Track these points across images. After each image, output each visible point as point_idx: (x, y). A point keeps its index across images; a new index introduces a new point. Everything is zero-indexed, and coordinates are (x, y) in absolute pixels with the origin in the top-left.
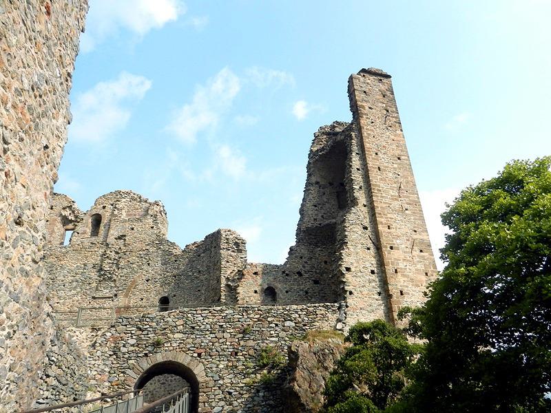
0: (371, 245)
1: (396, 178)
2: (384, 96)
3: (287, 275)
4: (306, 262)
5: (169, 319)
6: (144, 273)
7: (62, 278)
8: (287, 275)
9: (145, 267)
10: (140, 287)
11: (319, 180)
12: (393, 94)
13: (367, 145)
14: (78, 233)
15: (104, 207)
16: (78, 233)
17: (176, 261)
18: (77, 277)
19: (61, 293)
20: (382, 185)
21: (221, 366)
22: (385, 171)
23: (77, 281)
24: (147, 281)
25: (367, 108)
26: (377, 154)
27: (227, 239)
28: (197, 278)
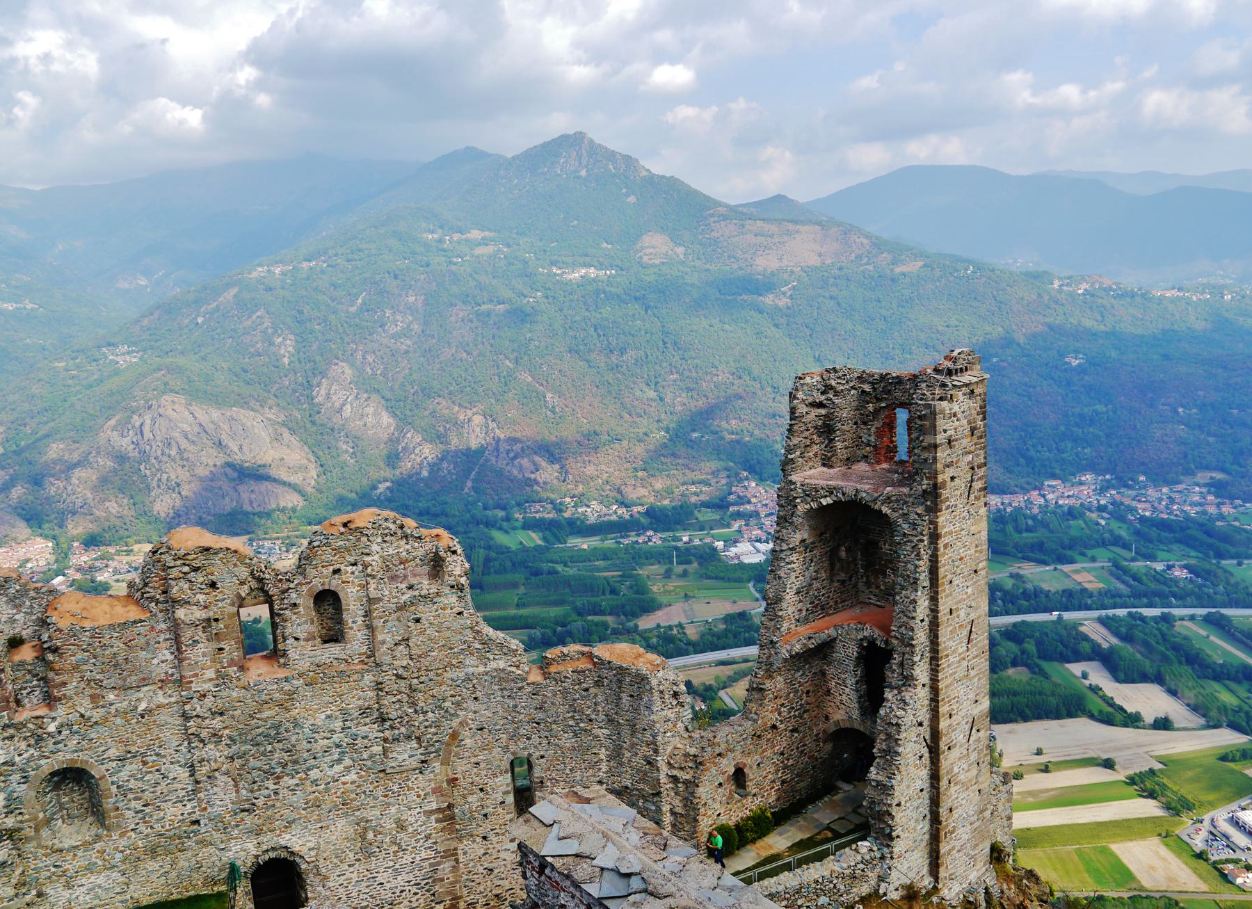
0: (925, 752)
3: (759, 737)
4: (782, 705)
6: (471, 715)
7: (306, 746)
9: (472, 705)
11: (806, 536)
13: (942, 571)
14: (297, 639)
16: (297, 639)
18: (336, 738)
19: (314, 774)
22: (958, 609)
23: (338, 746)
24: (481, 729)
27: (662, 692)
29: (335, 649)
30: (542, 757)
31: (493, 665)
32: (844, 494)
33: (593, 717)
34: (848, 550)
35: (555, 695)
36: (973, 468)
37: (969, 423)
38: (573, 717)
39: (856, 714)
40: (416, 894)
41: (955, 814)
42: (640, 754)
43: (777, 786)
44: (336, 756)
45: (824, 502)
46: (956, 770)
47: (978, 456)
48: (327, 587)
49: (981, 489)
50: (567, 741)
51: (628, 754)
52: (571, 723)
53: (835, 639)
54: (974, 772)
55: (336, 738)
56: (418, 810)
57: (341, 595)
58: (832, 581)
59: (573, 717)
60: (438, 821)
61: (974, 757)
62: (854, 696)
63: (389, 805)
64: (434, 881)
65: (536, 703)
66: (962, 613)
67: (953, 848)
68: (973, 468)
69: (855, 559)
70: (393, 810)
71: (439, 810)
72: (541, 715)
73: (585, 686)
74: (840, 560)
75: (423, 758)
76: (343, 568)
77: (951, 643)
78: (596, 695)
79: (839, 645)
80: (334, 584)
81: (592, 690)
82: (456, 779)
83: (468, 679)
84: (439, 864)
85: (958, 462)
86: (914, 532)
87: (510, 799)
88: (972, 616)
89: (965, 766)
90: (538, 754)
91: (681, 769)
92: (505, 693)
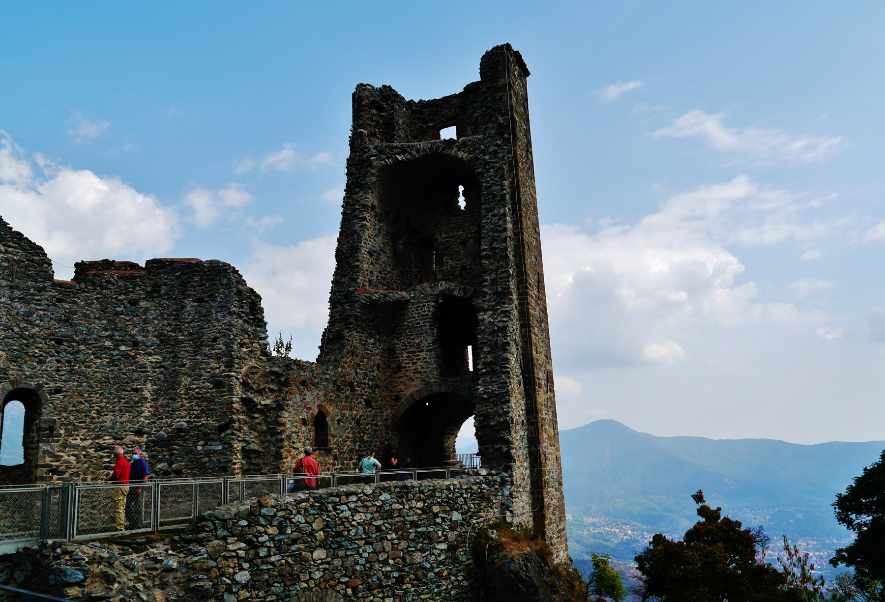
5: (300, 518)
17: (59, 300)
28: (126, 356)
30: (58, 391)
32: (418, 151)
33: (140, 338)
35: (90, 305)
42: (206, 375)
50: (99, 366)
52: (108, 343)
53: (409, 301)
59: (111, 337)
65: (60, 313)
72: (65, 330)
73: (132, 296)
79: (411, 308)
81: (143, 304)
86: (496, 159)
91: (260, 392)
92: (17, 293)
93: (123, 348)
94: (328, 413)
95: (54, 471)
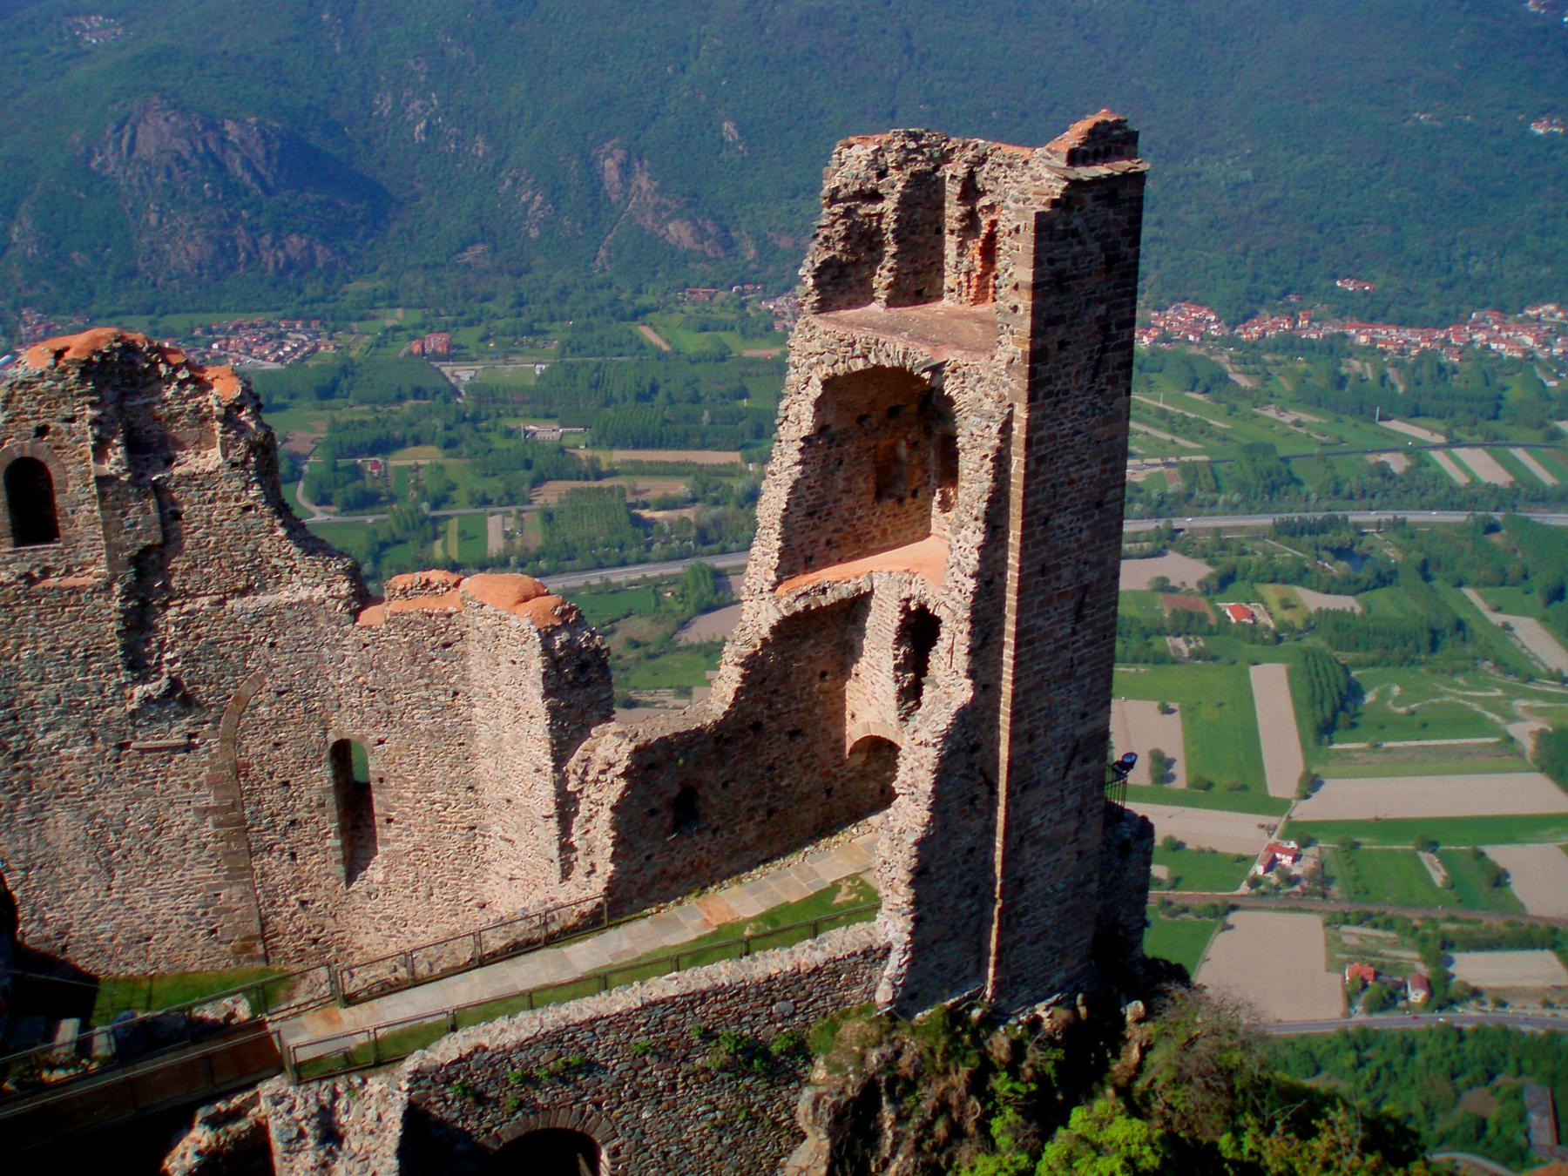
1: (1079, 575)
2: (1108, 270)
3: (727, 741)
4: (776, 691)
8: (727, 741)
10: (262, 709)
12: (1136, 242)
15: (42, 431)
18: (50, 689)
20: (1040, 622)
21: (645, 1115)
25: (1053, 347)
26: (1047, 520)
29: (47, 552)
30: (381, 742)
31: (304, 594)
33: (460, 687)
34: (913, 445)
36: (1105, 328)
37: (1104, 249)
38: (427, 686)
39: (892, 715)
40: (188, 927)
41: (1030, 889)
43: (760, 815)
44: (51, 719)
45: (860, 365)
46: (1036, 821)
47: (1120, 305)
48: (27, 454)
49: (1120, 366)
51: (510, 752)
52: (425, 694)
54: (1072, 825)
55: (50, 689)
56: (186, 806)
57: (53, 468)
58: (879, 496)
60: (217, 825)
61: (1071, 801)
62: (892, 689)
63: (138, 797)
64: (215, 911)
66: (1066, 573)
67: (1023, 938)
68: (1105, 328)
69: (923, 462)
70: (146, 805)
71: (215, 810)
74: (897, 460)
75: (191, 731)
76: (53, 425)
77: (1040, 622)
78: (464, 654)
80: (41, 450)
81: (458, 646)
82: (248, 766)
83: (258, 616)
84: (220, 886)
85: (1074, 316)
87: (331, 799)
88: (1090, 576)
89: (1057, 816)
90: (373, 737)
93: (442, 698)
94: (700, 784)
95: (389, 821)
